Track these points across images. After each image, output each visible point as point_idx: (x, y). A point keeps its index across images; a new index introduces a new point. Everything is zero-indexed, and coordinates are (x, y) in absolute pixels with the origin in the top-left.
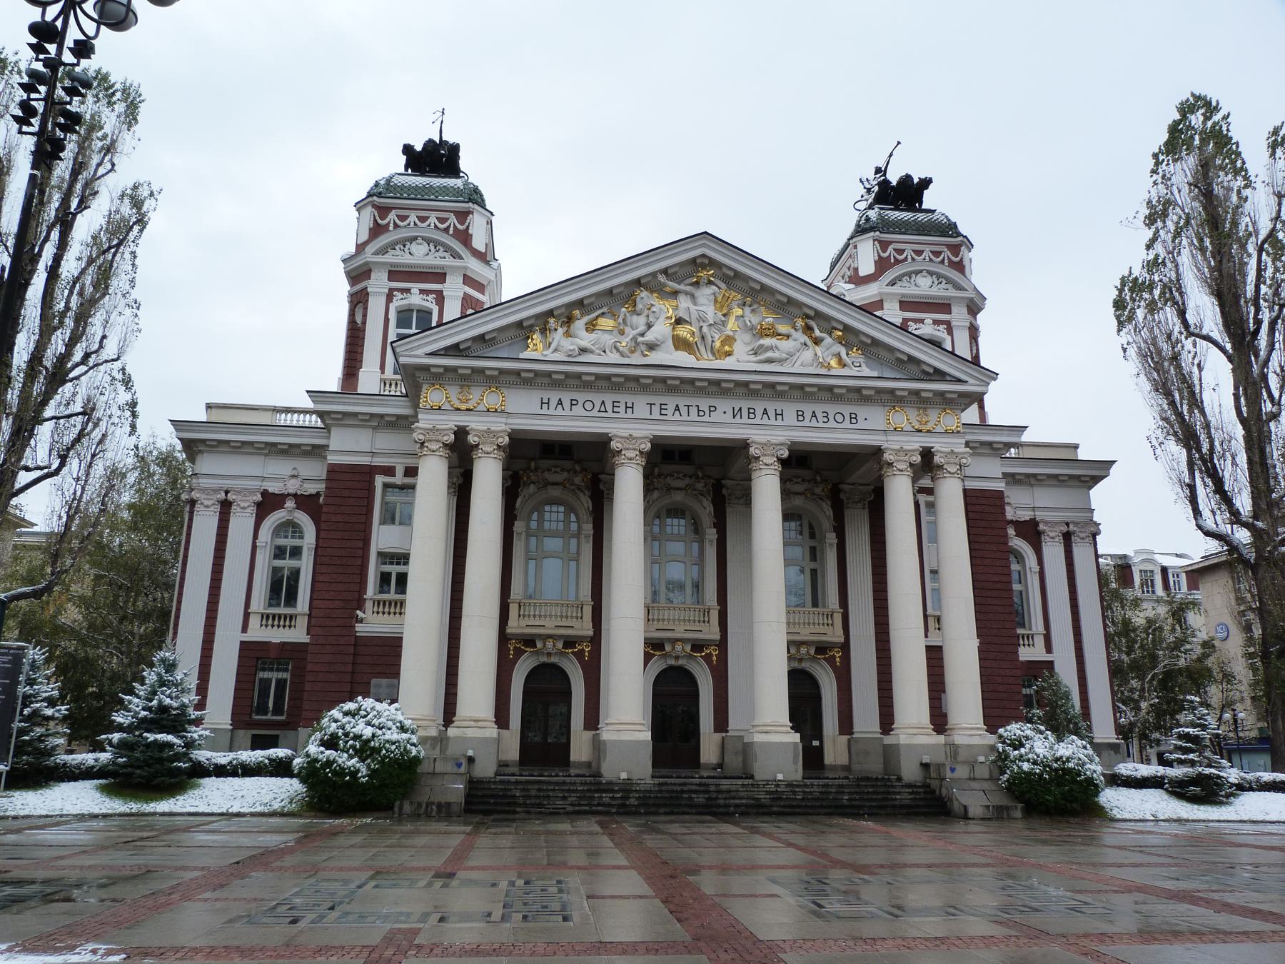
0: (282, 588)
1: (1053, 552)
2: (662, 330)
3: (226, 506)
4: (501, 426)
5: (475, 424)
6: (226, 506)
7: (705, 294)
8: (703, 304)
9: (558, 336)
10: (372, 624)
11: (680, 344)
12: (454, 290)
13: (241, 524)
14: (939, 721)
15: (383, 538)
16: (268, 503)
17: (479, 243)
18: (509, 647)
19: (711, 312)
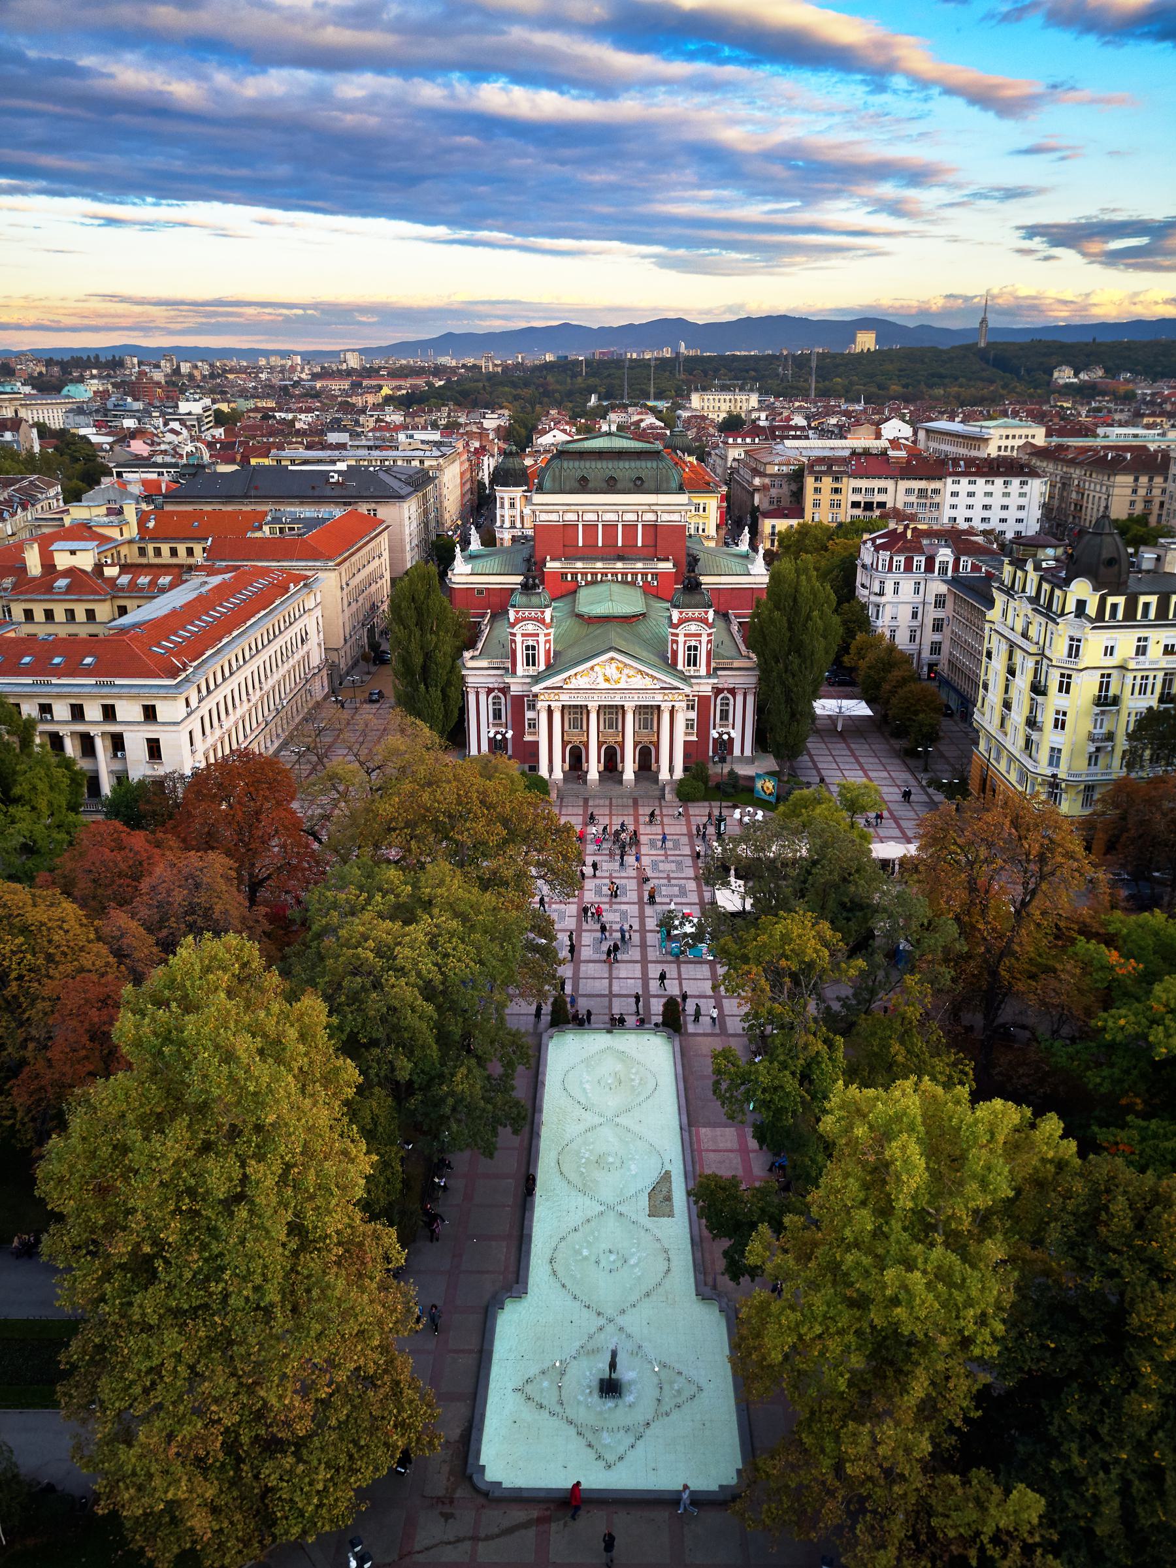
0: (497, 714)
1: (740, 698)
2: (601, 679)
3: (477, 693)
4: (559, 704)
5: (553, 704)
6: (477, 693)
7: (614, 665)
8: (611, 671)
9: (573, 680)
10: (527, 738)
11: (607, 680)
12: (542, 639)
13: (483, 697)
14: (671, 770)
15: (529, 715)
16: (490, 691)
17: (548, 620)
18: (564, 744)
19: (614, 671)
